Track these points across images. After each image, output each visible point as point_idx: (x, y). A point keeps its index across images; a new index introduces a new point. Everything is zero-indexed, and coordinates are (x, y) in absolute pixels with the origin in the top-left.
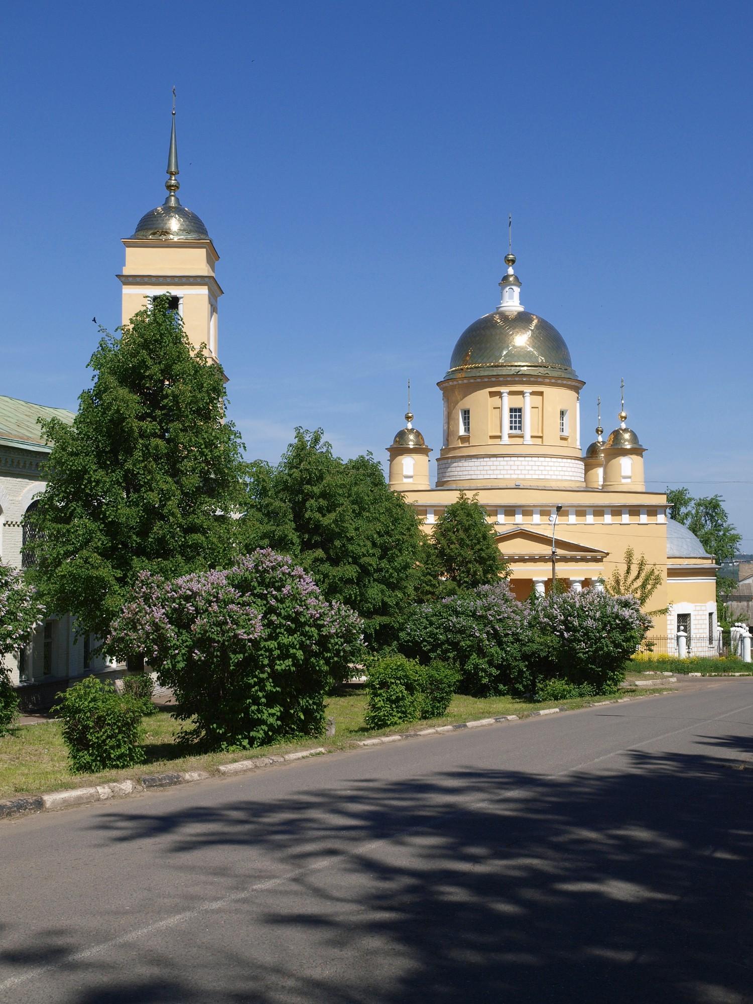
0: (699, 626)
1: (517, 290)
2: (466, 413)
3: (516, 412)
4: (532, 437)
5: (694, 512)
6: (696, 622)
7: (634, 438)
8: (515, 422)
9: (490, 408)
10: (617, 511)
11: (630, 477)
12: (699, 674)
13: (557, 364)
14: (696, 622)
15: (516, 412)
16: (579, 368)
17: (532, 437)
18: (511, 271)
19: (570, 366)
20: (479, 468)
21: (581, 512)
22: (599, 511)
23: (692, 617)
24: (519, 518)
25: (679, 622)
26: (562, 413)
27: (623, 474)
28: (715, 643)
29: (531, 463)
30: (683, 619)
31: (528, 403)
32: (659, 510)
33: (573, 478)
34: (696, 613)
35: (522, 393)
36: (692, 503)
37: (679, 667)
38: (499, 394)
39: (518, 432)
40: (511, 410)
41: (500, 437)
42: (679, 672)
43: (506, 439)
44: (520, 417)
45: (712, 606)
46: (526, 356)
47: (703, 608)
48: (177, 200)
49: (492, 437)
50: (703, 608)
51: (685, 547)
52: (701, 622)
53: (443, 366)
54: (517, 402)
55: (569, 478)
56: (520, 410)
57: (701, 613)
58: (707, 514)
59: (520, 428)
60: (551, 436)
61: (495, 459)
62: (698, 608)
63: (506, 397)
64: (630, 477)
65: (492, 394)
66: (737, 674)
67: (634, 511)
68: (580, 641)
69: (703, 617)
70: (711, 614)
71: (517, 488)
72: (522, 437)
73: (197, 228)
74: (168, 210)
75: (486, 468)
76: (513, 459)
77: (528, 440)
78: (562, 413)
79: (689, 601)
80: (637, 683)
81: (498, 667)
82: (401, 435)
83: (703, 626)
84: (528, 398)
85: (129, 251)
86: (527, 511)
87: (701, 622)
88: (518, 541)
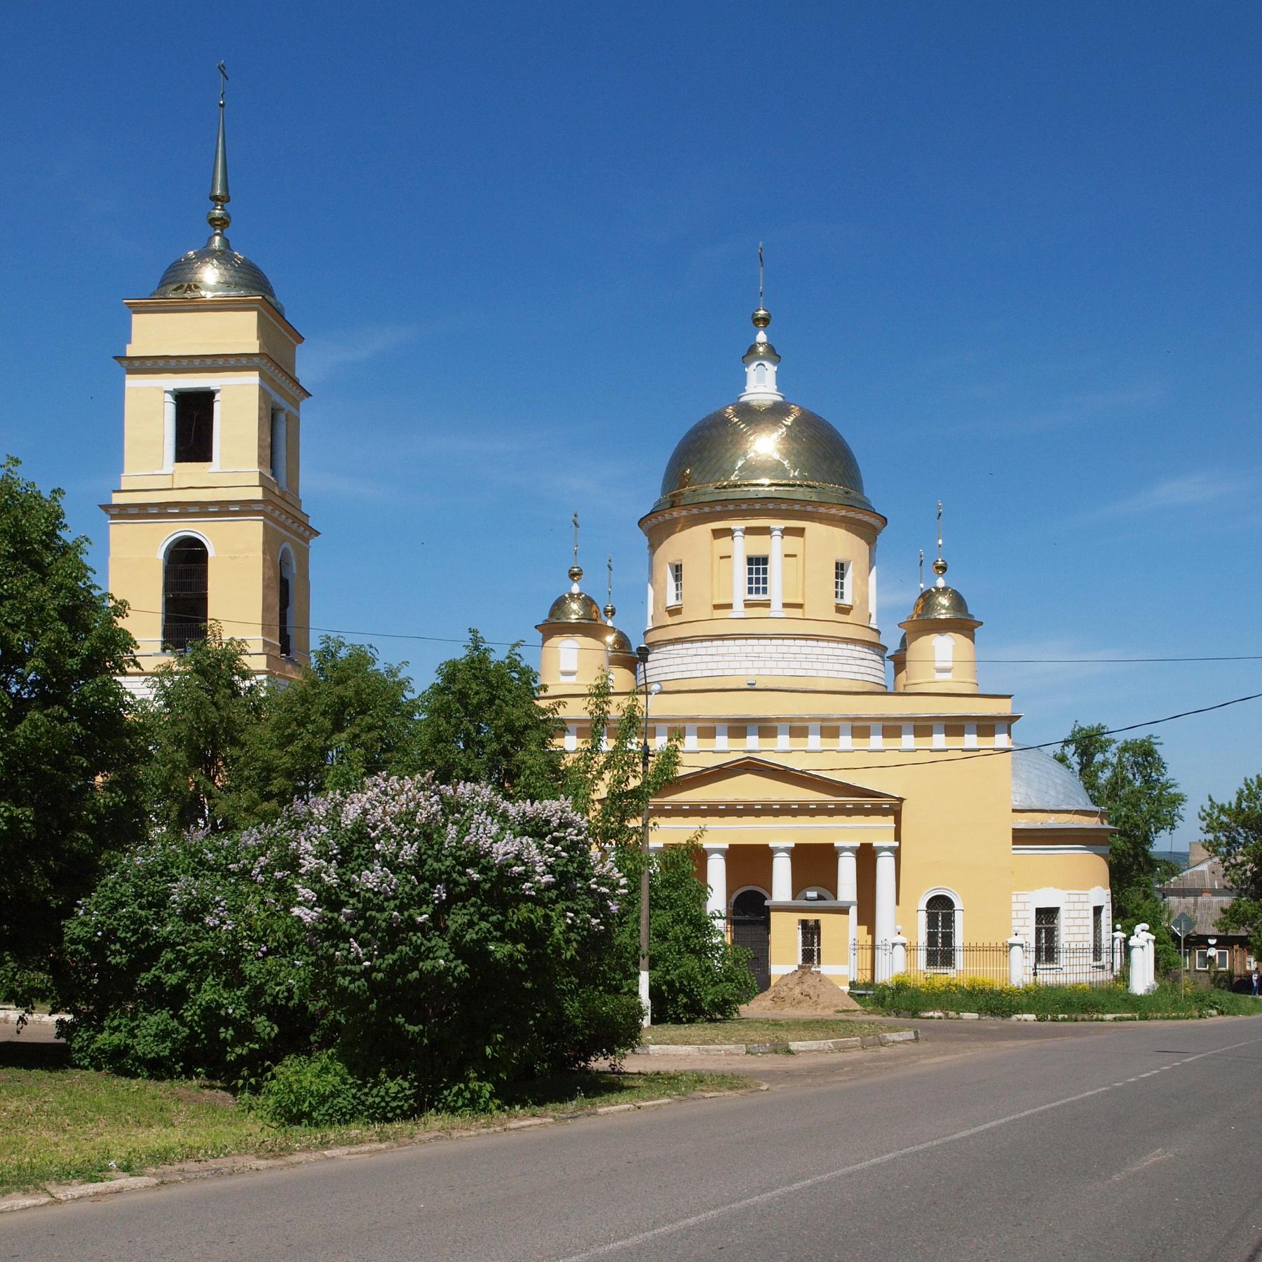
0: (1073, 931)
1: (771, 369)
2: (677, 570)
3: (757, 563)
4: (785, 605)
5: (1115, 761)
6: (1070, 922)
7: (959, 602)
8: (758, 580)
10: (923, 727)
12: (1032, 1017)
13: (833, 479)
14: (1070, 922)
15: (757, 563)
16: (875, 491)
17: (785, 605)
18: (761, 337)
19: (859, 489)
21: (861, 729)
22: (892, 728)
23: (1062, 914)
24: (752, 742)
25: (1038, 921)
26: (840, 569)
28: (1105, 958)
30: (1047, 916)
31: (774, 547)
32: (998, 725)
33: (859, 677)
34: (1070, 906)
35: (766, 531)
36: (1113, 748)
37: (997, 1003)
39: (761, 597)
40: (751, 561)
41: (729, 606)
42: (993, 1014)
43: (739, 610)
45: (1101, 895)
46: (776, 469)
47: (1083, 898)
48: (226, 242)
49: (716, 607)
50: (1083, 898)
51: (1052, 793)
52: (1078, 922)
53: (650, 494)
54: (757, 546)
55: (852, 676)
56: (765, 560)
57: (1079, 906)
58: (1136, 763)
59: (765, 590)
60: (821, 603)
61: (720, 643)
62: (1075, 898)
65: (717, 534)
66: (1109, 1017)
67: (955, 726)
68: (345, 937)
69: (1083, 914)
70: (1098, 911)
71: (752, 688)
72: (767, 605)
73: (253, 285)
74: (206, 254)
77: (776, 609)
78: (840, 569)
79: (1056, 886)
80: (794, 1046)
81: (276, 1012)
82: (559, 605)
83: (1083, 930)
85: (137, 319)
86: (766, 728)
87: (1078, 922)
88: (748, 779)
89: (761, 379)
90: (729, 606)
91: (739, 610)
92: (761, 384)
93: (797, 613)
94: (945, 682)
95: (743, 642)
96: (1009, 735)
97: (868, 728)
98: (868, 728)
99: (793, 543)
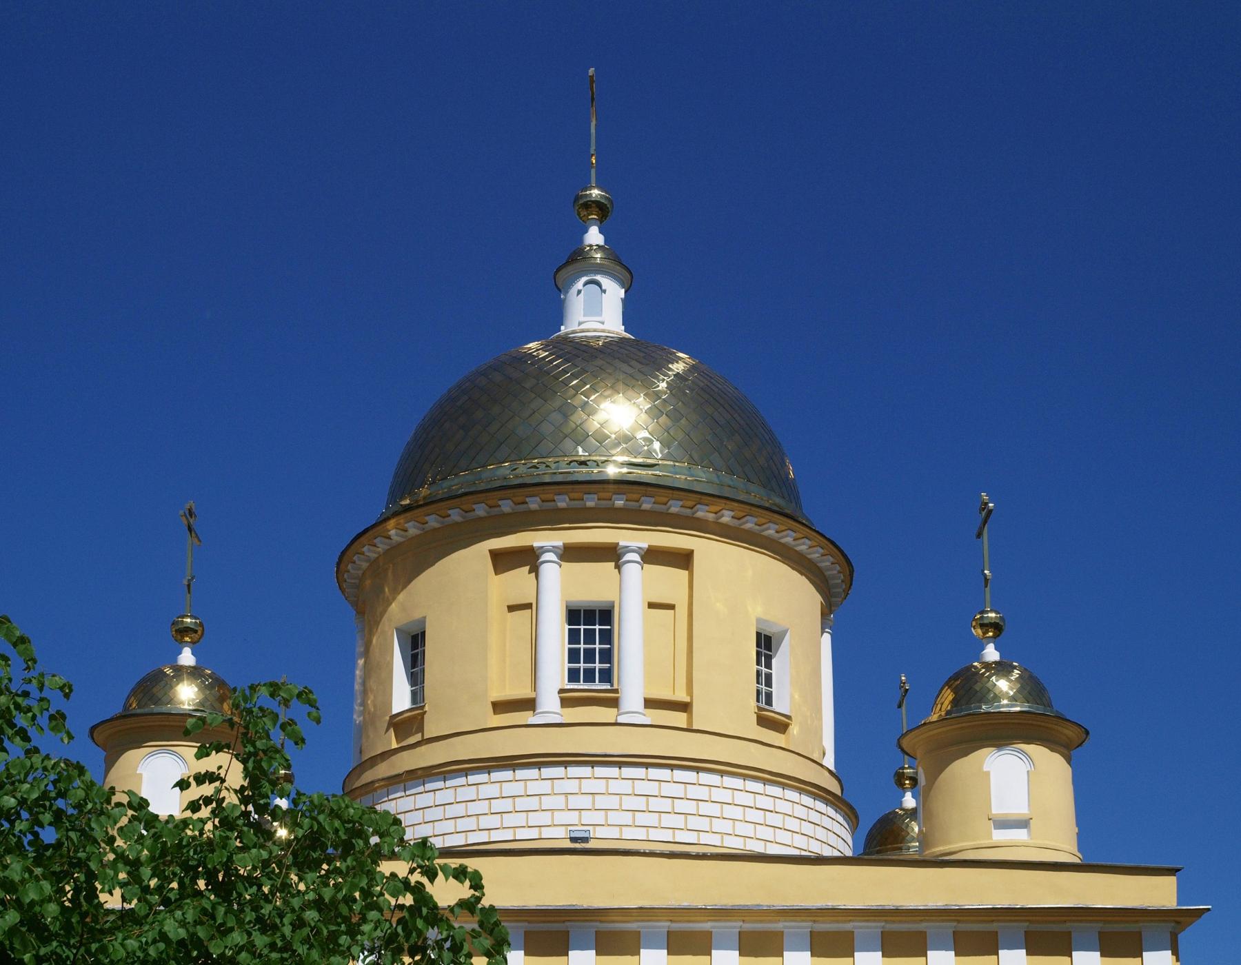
3: (592, 624)
4: (650, 703)
9: (496, 608)
11: (1023, 823)
15: (592, 624)
17: (650, 703)
20: (451, 811)
27: (997, 810)
29: (642, 787)
31: (632, 588)
38: (529, 558)
40: (574, 615)
41: (529, 704)
43: (550, 705)
44: (607, 637)
49: (500, 707)
54: (593, 582)
56: (604, 615)
59: (607, 676)
61: (507, 775)
63: (552, 571)
64: (1023, 823)
72: (614, 703)
75: (474, 808)
76: (574, 771)
84: (634, 571)
89: (594, 309)
90: (529, 704)
91: (550, 705)
92: (597, 309)
93: (679, 719)
94: (1015, 844)
95: (558, 771)
96: (1175, 953)
97: (849, 936)
98: (849, 936)
99: (669, 581)
